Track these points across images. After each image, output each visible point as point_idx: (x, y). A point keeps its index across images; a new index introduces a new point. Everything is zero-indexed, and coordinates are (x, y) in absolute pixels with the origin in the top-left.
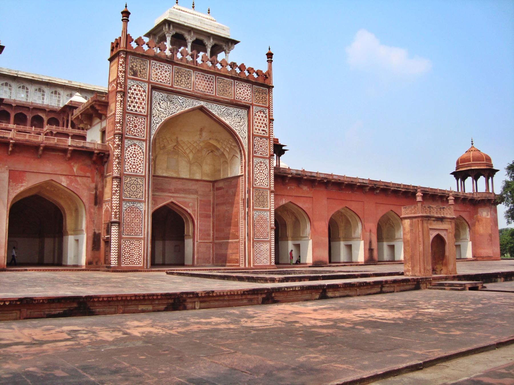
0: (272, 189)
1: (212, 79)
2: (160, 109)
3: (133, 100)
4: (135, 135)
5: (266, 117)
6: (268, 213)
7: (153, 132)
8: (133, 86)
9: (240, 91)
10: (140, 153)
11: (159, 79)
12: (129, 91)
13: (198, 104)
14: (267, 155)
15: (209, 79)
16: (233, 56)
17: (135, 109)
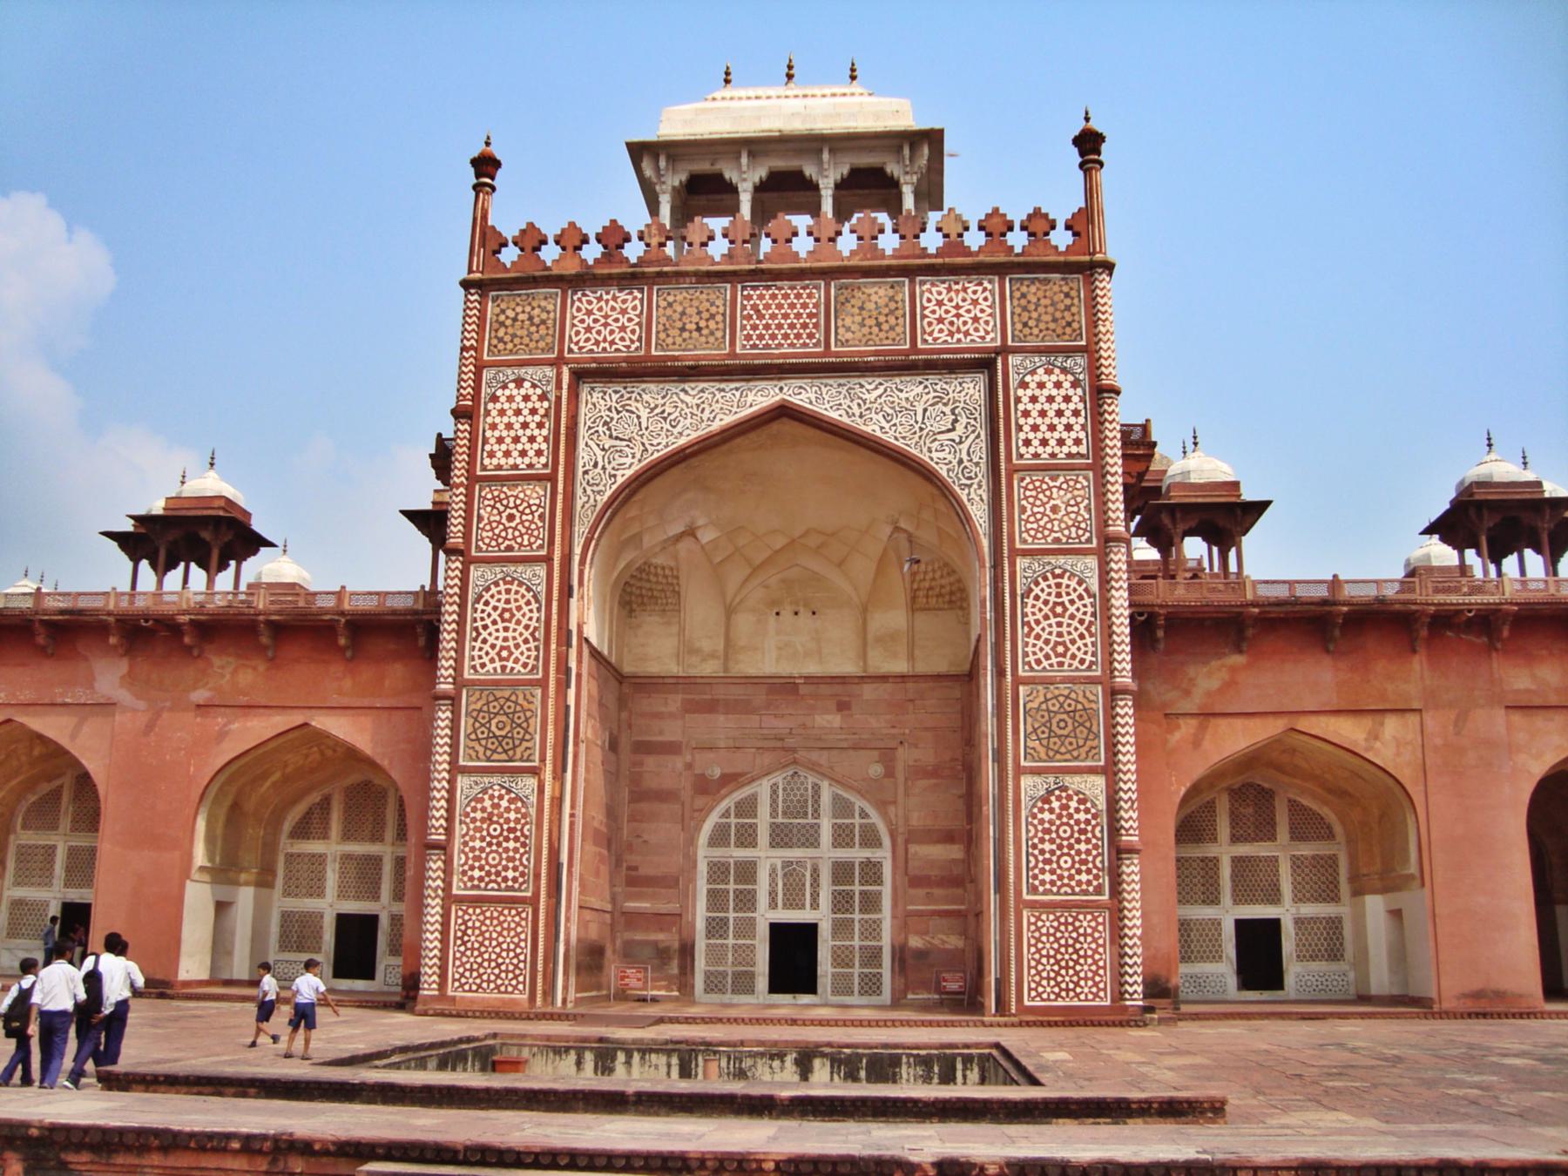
0: (1124, 674)
1: (810, 296)
2: (608, 443)
3: (505, 433)
4: (510, 548)
5: (1075, 384)
6: (1100, 781)
7: (581, 530)
8: (505, 387)
9: (940, 312)
10: (528, 603)
12: (490, 406)
13: (761, 397)
14: (1089, 541)
15: (798, 296)
16: (970, 192)
17: (511, 461)
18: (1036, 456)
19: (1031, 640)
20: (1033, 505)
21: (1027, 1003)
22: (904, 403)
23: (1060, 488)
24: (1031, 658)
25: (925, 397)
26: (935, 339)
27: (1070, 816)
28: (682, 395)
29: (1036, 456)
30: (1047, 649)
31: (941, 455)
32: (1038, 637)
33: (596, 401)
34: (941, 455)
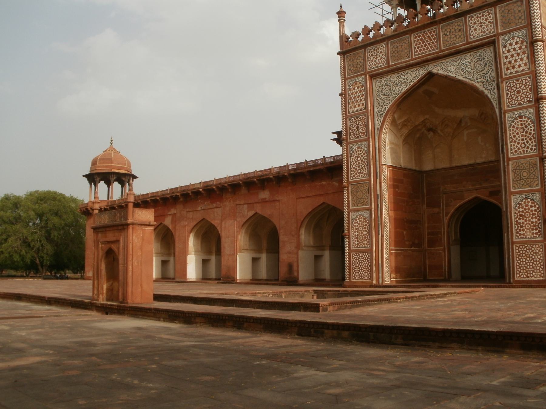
11: (375, 65)
18: (511, 73)
19: (513, 144)
20: (511, 92)
21: (516, 279)
22: (467, 64)
23: (520, 84)
24: (513, 151)
25: (474, 60)
26: (474, 37)
27: (529, 209)
28: (402, 76)
29: (511, 73)
30: (519, 146)
31: (481, 80)
32: (515, 142)
33: (377, 84)
34: (481, 80)
